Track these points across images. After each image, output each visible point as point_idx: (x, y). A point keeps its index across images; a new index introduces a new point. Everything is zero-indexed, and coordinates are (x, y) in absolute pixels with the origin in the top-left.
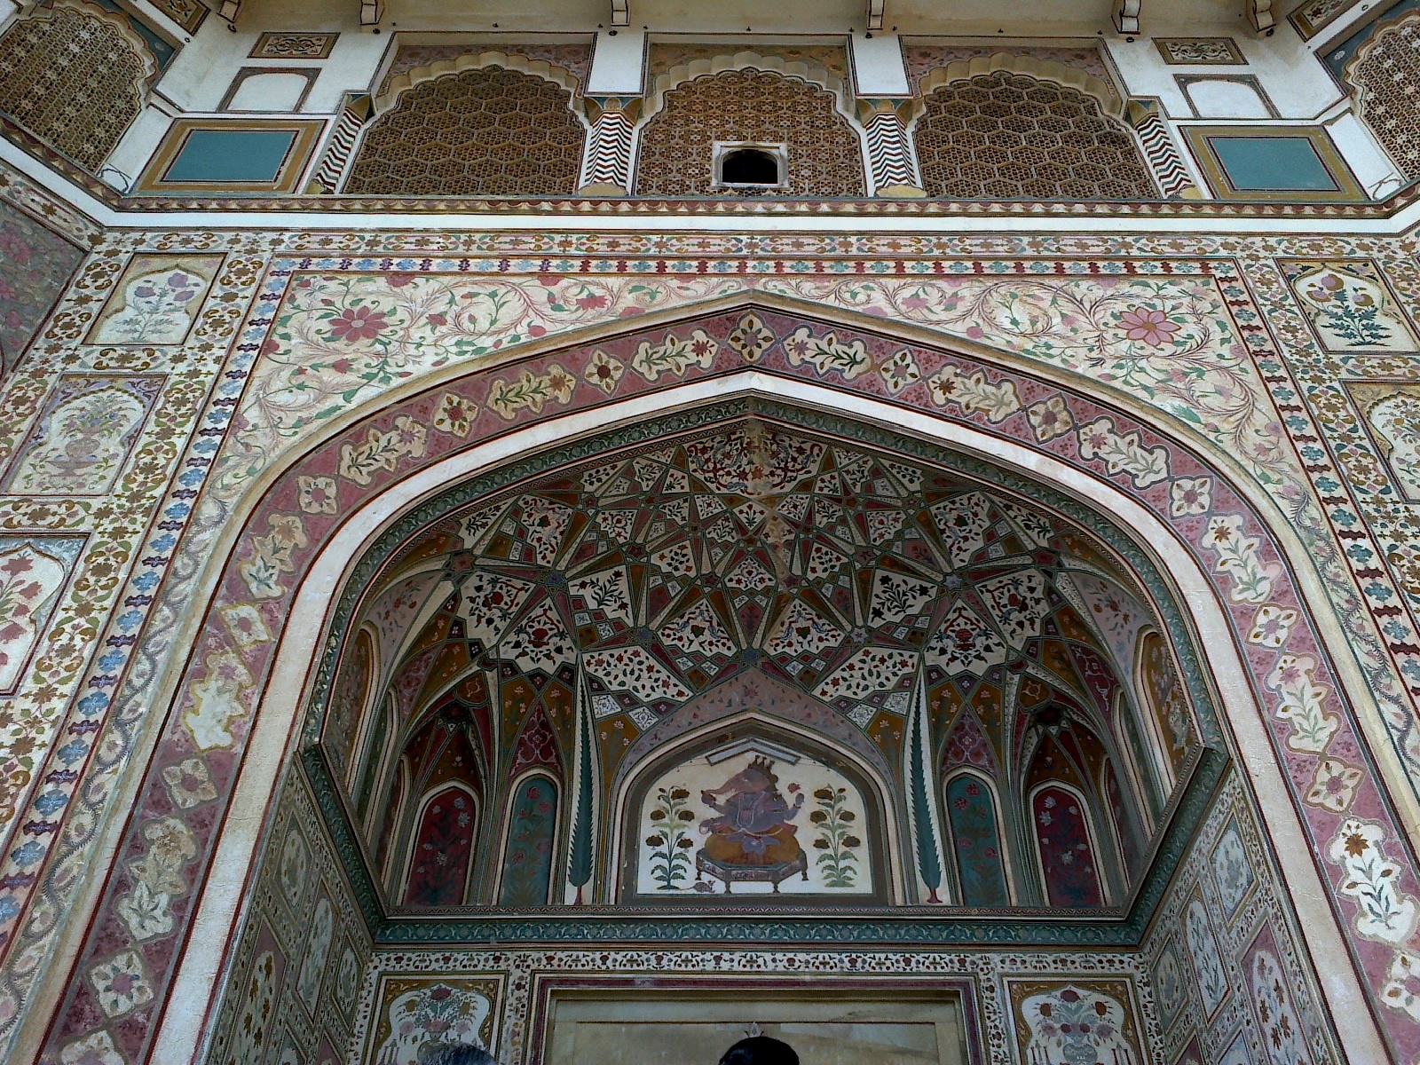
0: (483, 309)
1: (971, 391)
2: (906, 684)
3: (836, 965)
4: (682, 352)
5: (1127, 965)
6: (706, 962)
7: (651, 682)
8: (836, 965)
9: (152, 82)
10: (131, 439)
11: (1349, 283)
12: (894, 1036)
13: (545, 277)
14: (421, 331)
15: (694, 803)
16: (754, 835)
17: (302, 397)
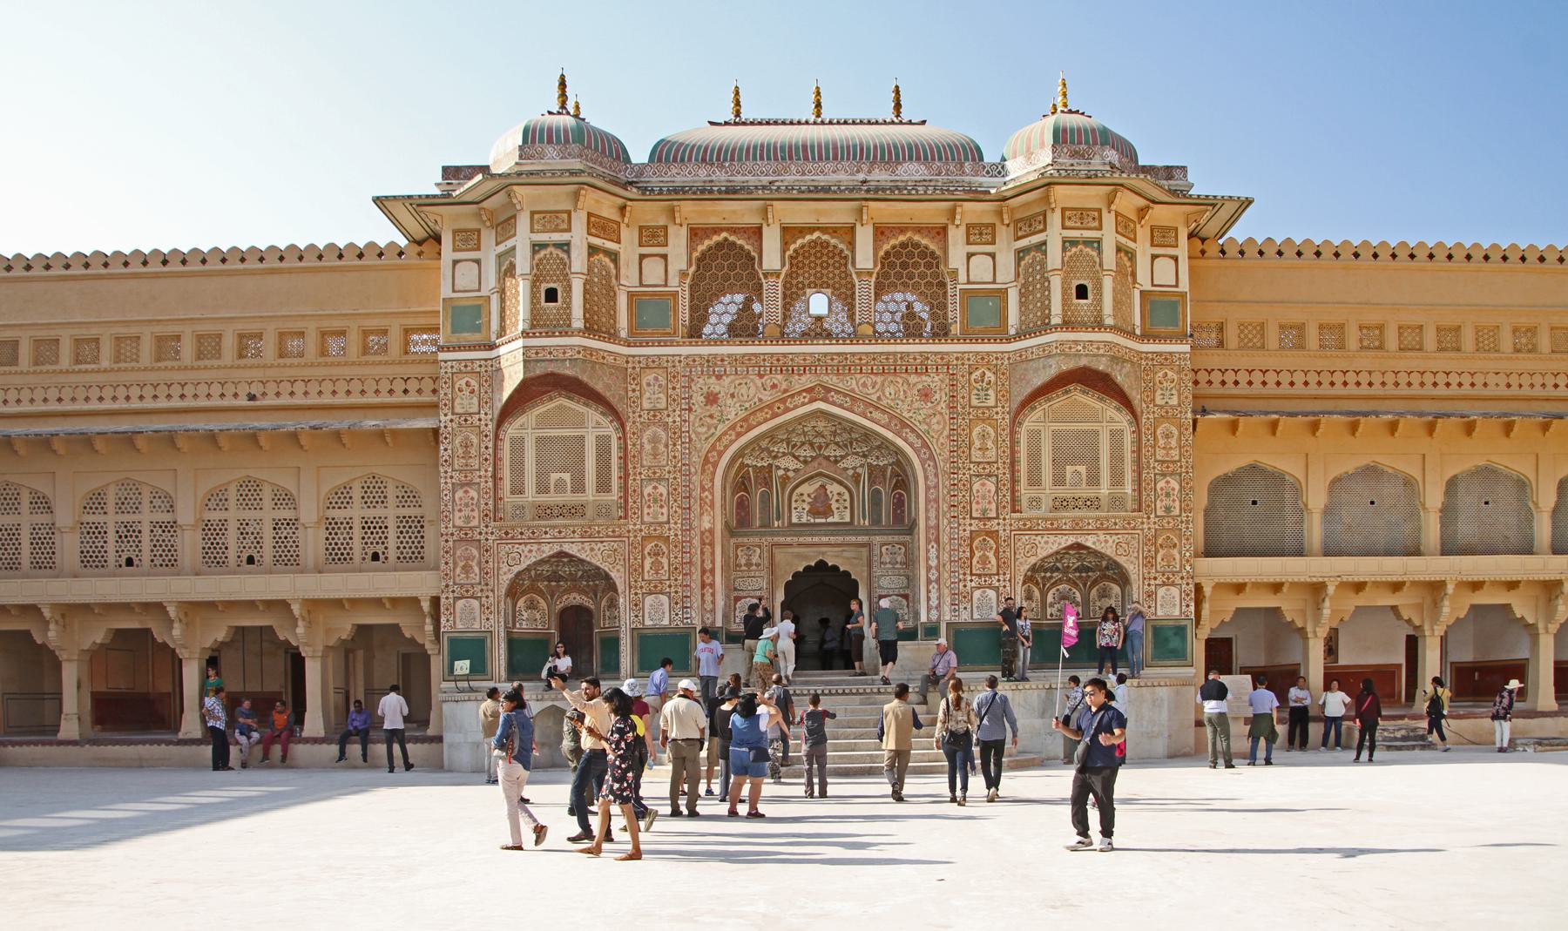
0: (744, 390)
1: (877, 415)
2: (862, 466)
3: (840, 539)
4: (799, 400)
5: (908, 538)
6: (809, 539)
7: (790, 463)
8: (840, 539)
9: (618, 277)
10: (667, 446)
11: (988, 374)
12: (852, 555)
13: (761, 376)
14: (729, 401)
15: (805, 497)
16: (821, 506)
17: (703, 430)
